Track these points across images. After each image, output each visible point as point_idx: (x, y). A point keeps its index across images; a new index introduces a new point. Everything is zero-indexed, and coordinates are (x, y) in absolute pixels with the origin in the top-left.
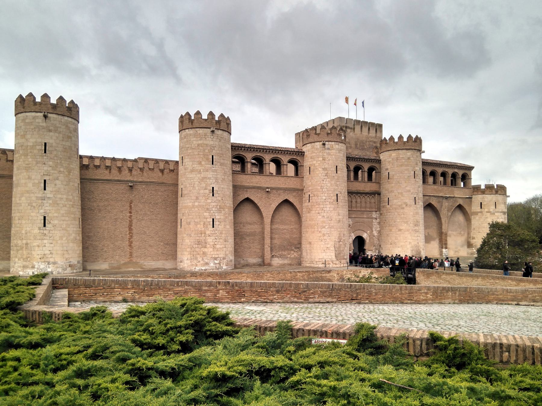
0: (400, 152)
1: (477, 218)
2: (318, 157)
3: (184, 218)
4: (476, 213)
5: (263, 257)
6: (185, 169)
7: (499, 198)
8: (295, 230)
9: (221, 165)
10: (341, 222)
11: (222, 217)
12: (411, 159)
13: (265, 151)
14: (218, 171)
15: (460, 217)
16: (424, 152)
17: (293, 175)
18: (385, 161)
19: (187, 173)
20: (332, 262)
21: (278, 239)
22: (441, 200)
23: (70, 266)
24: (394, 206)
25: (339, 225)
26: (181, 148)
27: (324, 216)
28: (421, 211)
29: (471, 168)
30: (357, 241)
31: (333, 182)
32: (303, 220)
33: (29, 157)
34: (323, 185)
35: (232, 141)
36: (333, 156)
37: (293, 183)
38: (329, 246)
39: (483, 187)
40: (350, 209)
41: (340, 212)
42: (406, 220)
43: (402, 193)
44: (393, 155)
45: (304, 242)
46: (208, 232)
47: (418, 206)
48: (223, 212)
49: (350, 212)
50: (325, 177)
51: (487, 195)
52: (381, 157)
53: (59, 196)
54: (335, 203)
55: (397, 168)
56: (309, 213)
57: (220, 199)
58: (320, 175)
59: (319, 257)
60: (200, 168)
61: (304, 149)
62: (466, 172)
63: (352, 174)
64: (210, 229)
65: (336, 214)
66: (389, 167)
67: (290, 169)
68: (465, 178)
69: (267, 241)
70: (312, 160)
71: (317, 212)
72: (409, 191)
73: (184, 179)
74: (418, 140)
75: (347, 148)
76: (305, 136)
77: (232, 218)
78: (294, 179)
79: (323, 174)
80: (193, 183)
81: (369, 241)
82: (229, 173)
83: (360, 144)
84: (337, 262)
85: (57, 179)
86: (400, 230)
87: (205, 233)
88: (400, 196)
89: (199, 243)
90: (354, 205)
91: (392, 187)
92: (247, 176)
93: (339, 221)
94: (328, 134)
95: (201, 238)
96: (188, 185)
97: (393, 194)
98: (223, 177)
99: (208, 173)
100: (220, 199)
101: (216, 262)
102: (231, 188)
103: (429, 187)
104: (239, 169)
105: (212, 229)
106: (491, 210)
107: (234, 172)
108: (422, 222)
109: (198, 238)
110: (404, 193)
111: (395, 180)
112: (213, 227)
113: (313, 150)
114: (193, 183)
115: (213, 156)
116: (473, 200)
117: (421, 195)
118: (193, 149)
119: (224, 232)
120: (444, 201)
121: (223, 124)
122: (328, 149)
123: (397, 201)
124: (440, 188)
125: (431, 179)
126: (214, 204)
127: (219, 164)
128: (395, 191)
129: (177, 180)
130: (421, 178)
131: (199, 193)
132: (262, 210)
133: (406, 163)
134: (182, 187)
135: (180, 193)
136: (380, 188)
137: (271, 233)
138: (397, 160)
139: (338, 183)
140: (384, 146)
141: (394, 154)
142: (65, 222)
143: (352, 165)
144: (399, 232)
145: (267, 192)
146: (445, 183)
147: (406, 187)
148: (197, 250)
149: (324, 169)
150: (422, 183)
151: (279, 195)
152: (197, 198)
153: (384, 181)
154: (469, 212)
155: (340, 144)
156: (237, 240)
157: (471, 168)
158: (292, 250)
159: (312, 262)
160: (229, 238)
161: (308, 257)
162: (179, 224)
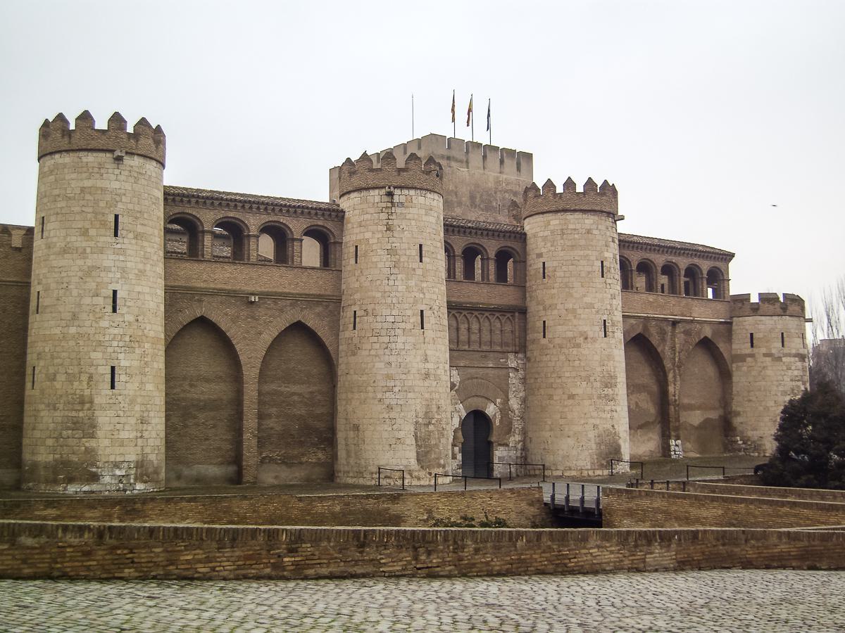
0: (569, 216)
1: (745, 368)
2: (377, 224)
3: (42, 363)
4: (742, 358)
5: (237, 459)
6: (49, 247)
7: (789, 323)
8: (319, 397)
9: (136, 238)
10: (432, 377)
11: (136, 363)
12: (595, 232)
13: (247, 206)
14: (129, 252)
15: (703, 368)
16: (622, 218)
17: (318, 265)
18: (535, 236)
19: (52, 257)
20: (410, 473)
21: (278, 417)
22: (664, 325)
24: (557, 341)
25: (426, 384)
26: (42, 198)
27: (390, 363)
28: (619, 354)
29: (729, 256)
30: (472, 420)
31: (412, 283)
32: (339, 373)
34: (387, 288)
35: (167, 182)
36: (413, 223)
37: (316, 284)
38: (401, 435)
39: (754, 299)
40: (454, 347)
41: (429, 353)
42: (583, 374)
43: (574, 311)
44: (552, 223)
45: (341, 424)
46: (97, 400)
47: (613, 341)
48: (137, 351)
49: (456, 354)
50: (393, 271)
51: (763, 318)
52: (527, 228)
54: (418, 330)
55: (562, 254)
56: (354, 354)
58: (380, 265)
59: (376, 463)
60: (84, 244)
61: (344, 204)
62: (718, 264)
63: (459, 265)
64: (103, 392)
65: (418, 359)
66: (543, 250)
67: (310, 252)
68: (718, 278)
69: (250, 422)
70: (362, 229)
71: (373, 352)
72: (591, 306)
73: (45, 271)
74: (609, 191)
75: (447, 204)
76: (352, 175)
77: (162, 366)
78: (319, 273)
79: (388, 264)
80: (65, 280)
81: (501, 421)
82: (155, 258)
83: (480, 198)
84: (422, 474)
86: (572, 397)
87: (91, 402)
88: (570, 316)
89: (76, 424)
90: (463, 337)
91: (552, 297)
92: (202, 266)
93: (427, 375)
94: (400, 170)
95: (81, 414)
96: (53, 286)
97: (555, 312)
98: (141, 266)
99: (104, 257)
101: (118, 472)
102: (161, 293)
103: (636, 297)
104: (183, 248)
105: (110, 392)
106: (774, 351)
107: (169, 256)
108: (622, 378)
109: (74, 414)
110: (579, 311)
111: (559, 280)
112: (113, 387)
113: (364, 206)
115: (116, 217)
116: (734, 327)
117: (618, 316)
118: (70, 198)
119: (139, 400)
121: (146, 141)
122: (402, 204)
123: (565, 328)
124: (661, 300)
125: (640, 281)
126: (116, 331)
127: (131, 235)
128: (559, 306)
129: (27, 272)
130: (618, 276)
131: (80, 305)
132: (238, 347)
133: (583, 242)
134: (39, 288)
135: (33, 304)
136: (524, 298)
137: (261, 403)
138: (563, 234)
139: (424, 285)
140: (531, 202)
141: (555, 221)
143: (459, 244)
144: (571, 402)
145: (252, 303)
146: (673, 290)
147: (585, 296)
148: (70, 441)
149: (391, 252)
150: (619, 288)
151: (281, 311)
152: (75, 317)
153: (533, 282)
154: (726, 355)
155: (429, 195)
156: (174, 420)
157: (729, 256)
158: (314, 445)
159: (360, 474)
160: (152, 414)
161: (352, 461)
162: (29, 378)
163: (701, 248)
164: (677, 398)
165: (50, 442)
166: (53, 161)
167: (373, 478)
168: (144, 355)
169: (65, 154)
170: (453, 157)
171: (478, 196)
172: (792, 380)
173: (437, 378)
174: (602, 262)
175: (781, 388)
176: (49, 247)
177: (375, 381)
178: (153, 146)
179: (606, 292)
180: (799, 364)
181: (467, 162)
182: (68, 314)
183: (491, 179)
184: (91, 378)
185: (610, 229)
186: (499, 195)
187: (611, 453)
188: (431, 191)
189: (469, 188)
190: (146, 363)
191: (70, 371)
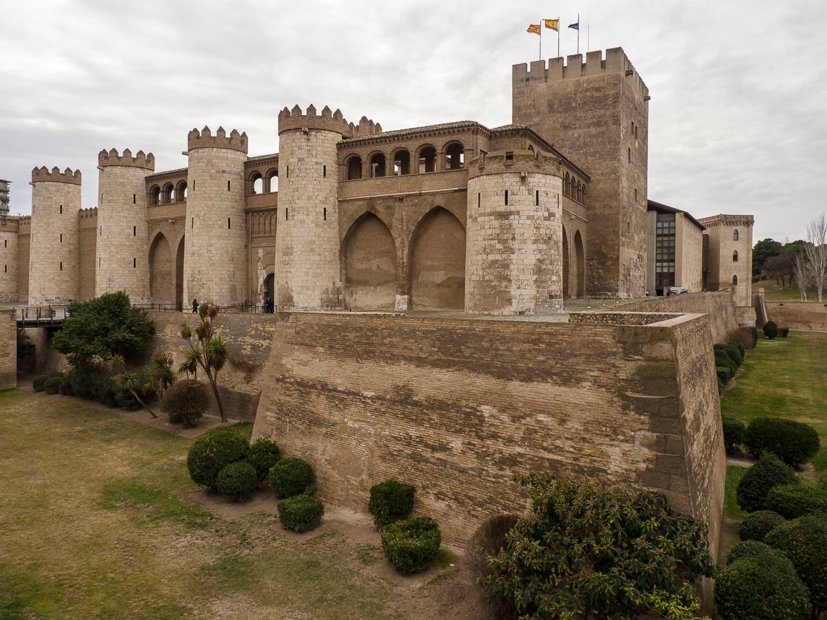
10: (196, 255)
22: (391, 203)
23: (46, 300)
25: (193, 258)
41: (194, 241)
53: (39, 246)
57: (105, 237)
85: (39, 232)
92: (160, 208)
93: (193, 254)
98: (110, 214)
100: (105, 237)
106: (473, 213)
120: (397, 204)
142: (43, 266)
155: (200, 150)
163: (445, 127)
164: (405, 261)
168: (110, 252)
170: (532, 78)
171: (557, 102)
172: (484, 239)
173: (200, 255)
174: (288, 167)
175: (475, 249)
178: (116, 160)
179: (289, 188)
180: (496, 223)
181: (546, 77)
183: (571, 84)
185: (296, 141)
186: (579, 95)
187: (284, 301)
188: (201, 148)
189: (547, 98)
190: (112, 256)
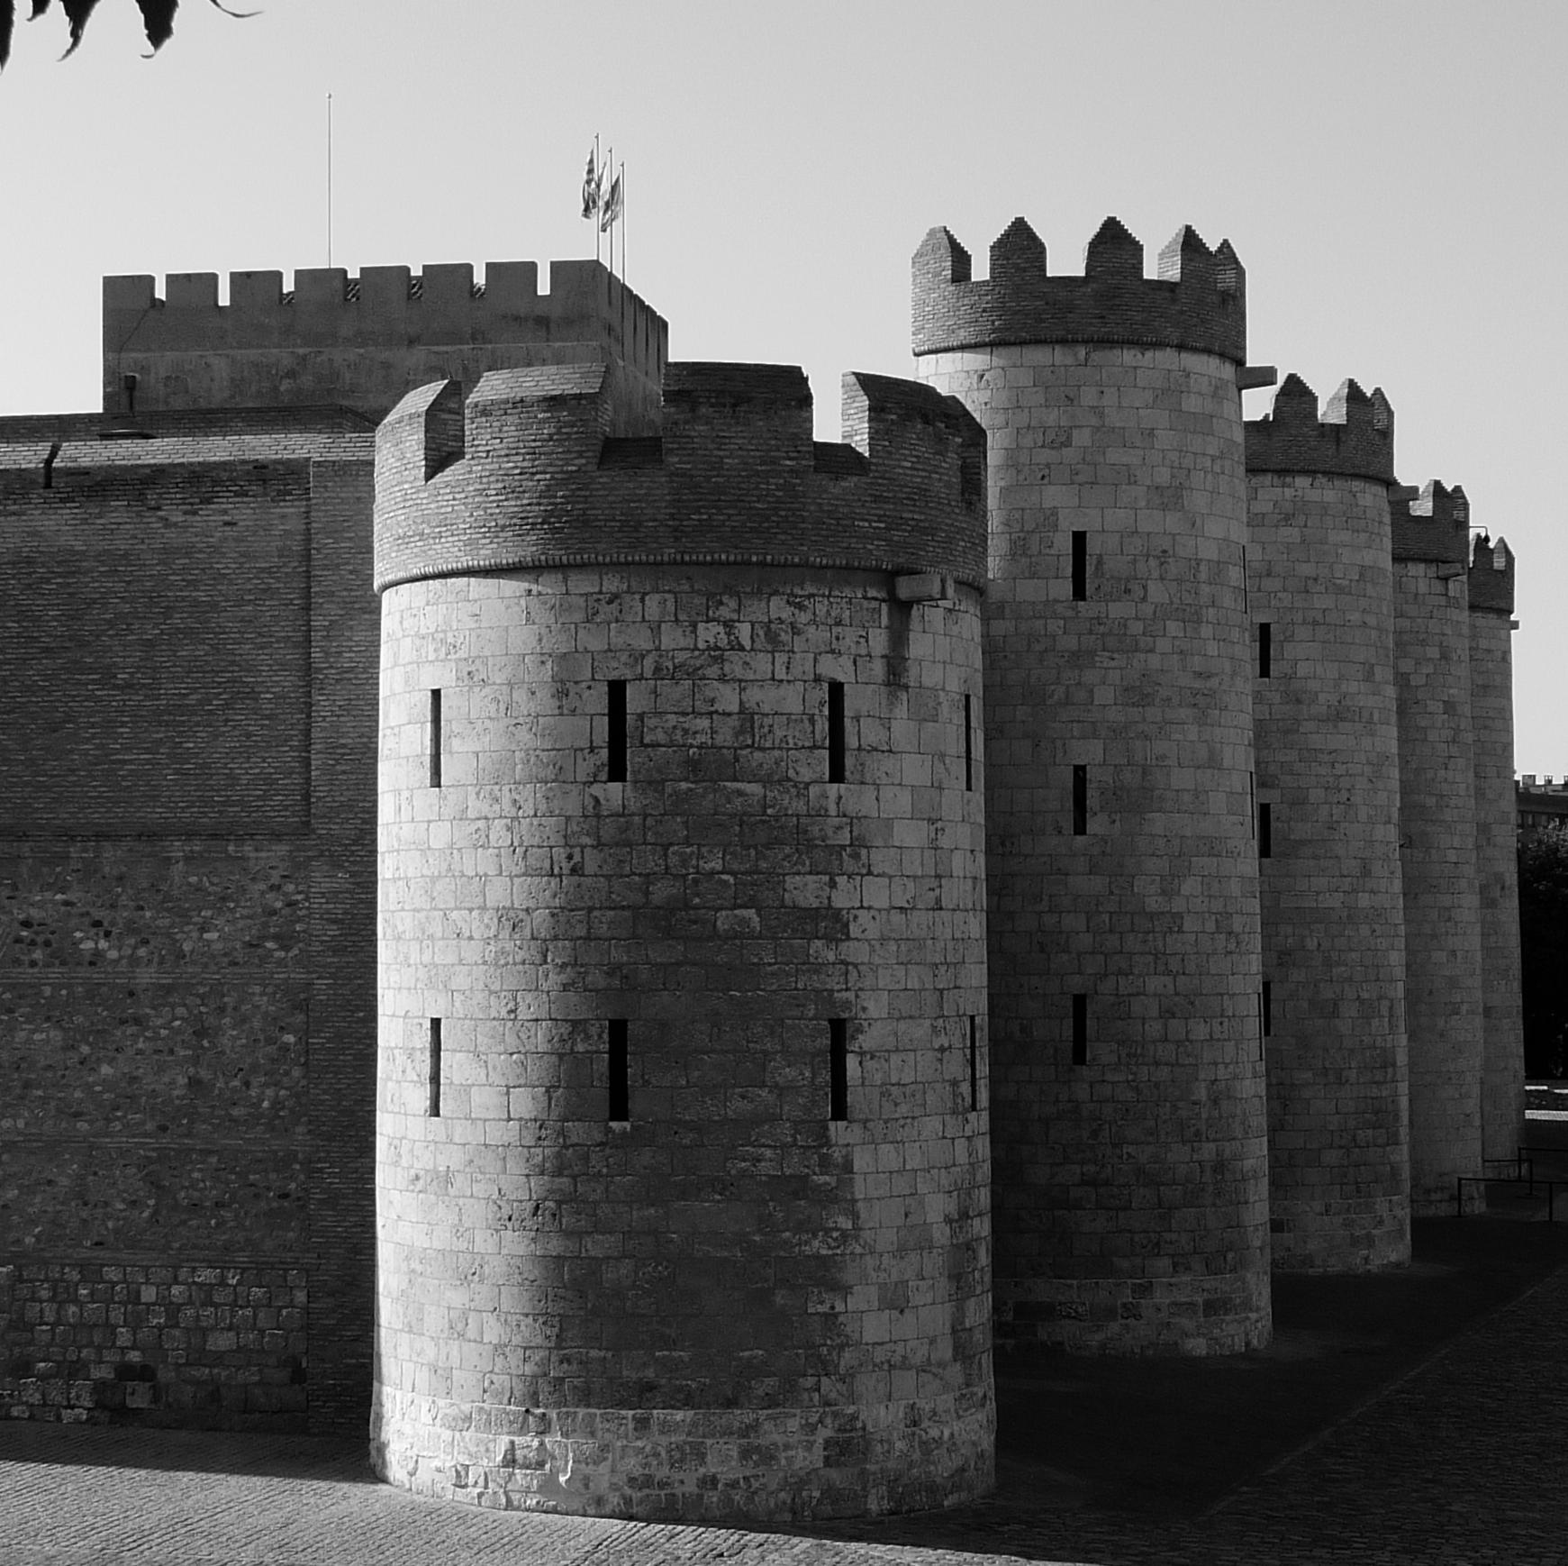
2: (1423, 643)
33: (1206, 631)
50: (1454, 750)
58: (1432, 736)
80: (1345, 783)
96: (1316, 795)
109: (1375, 1092)
114: (1345, 783)
152: (1366, 872)
165: (1331, 1157)
166: (1289, 492)
167: (1431, 1202)
169: (1321, 480)
176: (1299, 701)
177: (1431, 992)
182: (1354, 863)
184: (1391, 1008)
191: (1365, 995)
